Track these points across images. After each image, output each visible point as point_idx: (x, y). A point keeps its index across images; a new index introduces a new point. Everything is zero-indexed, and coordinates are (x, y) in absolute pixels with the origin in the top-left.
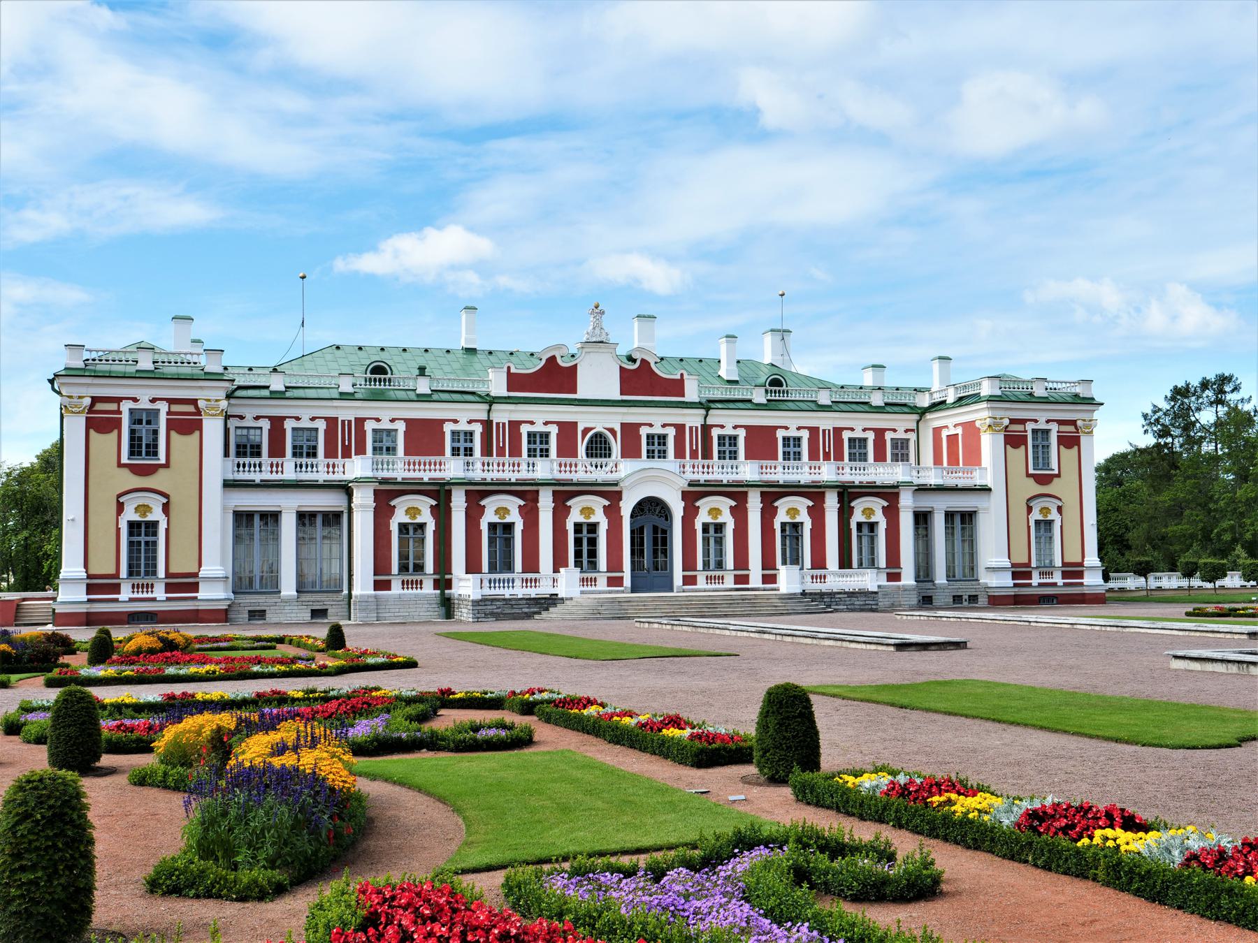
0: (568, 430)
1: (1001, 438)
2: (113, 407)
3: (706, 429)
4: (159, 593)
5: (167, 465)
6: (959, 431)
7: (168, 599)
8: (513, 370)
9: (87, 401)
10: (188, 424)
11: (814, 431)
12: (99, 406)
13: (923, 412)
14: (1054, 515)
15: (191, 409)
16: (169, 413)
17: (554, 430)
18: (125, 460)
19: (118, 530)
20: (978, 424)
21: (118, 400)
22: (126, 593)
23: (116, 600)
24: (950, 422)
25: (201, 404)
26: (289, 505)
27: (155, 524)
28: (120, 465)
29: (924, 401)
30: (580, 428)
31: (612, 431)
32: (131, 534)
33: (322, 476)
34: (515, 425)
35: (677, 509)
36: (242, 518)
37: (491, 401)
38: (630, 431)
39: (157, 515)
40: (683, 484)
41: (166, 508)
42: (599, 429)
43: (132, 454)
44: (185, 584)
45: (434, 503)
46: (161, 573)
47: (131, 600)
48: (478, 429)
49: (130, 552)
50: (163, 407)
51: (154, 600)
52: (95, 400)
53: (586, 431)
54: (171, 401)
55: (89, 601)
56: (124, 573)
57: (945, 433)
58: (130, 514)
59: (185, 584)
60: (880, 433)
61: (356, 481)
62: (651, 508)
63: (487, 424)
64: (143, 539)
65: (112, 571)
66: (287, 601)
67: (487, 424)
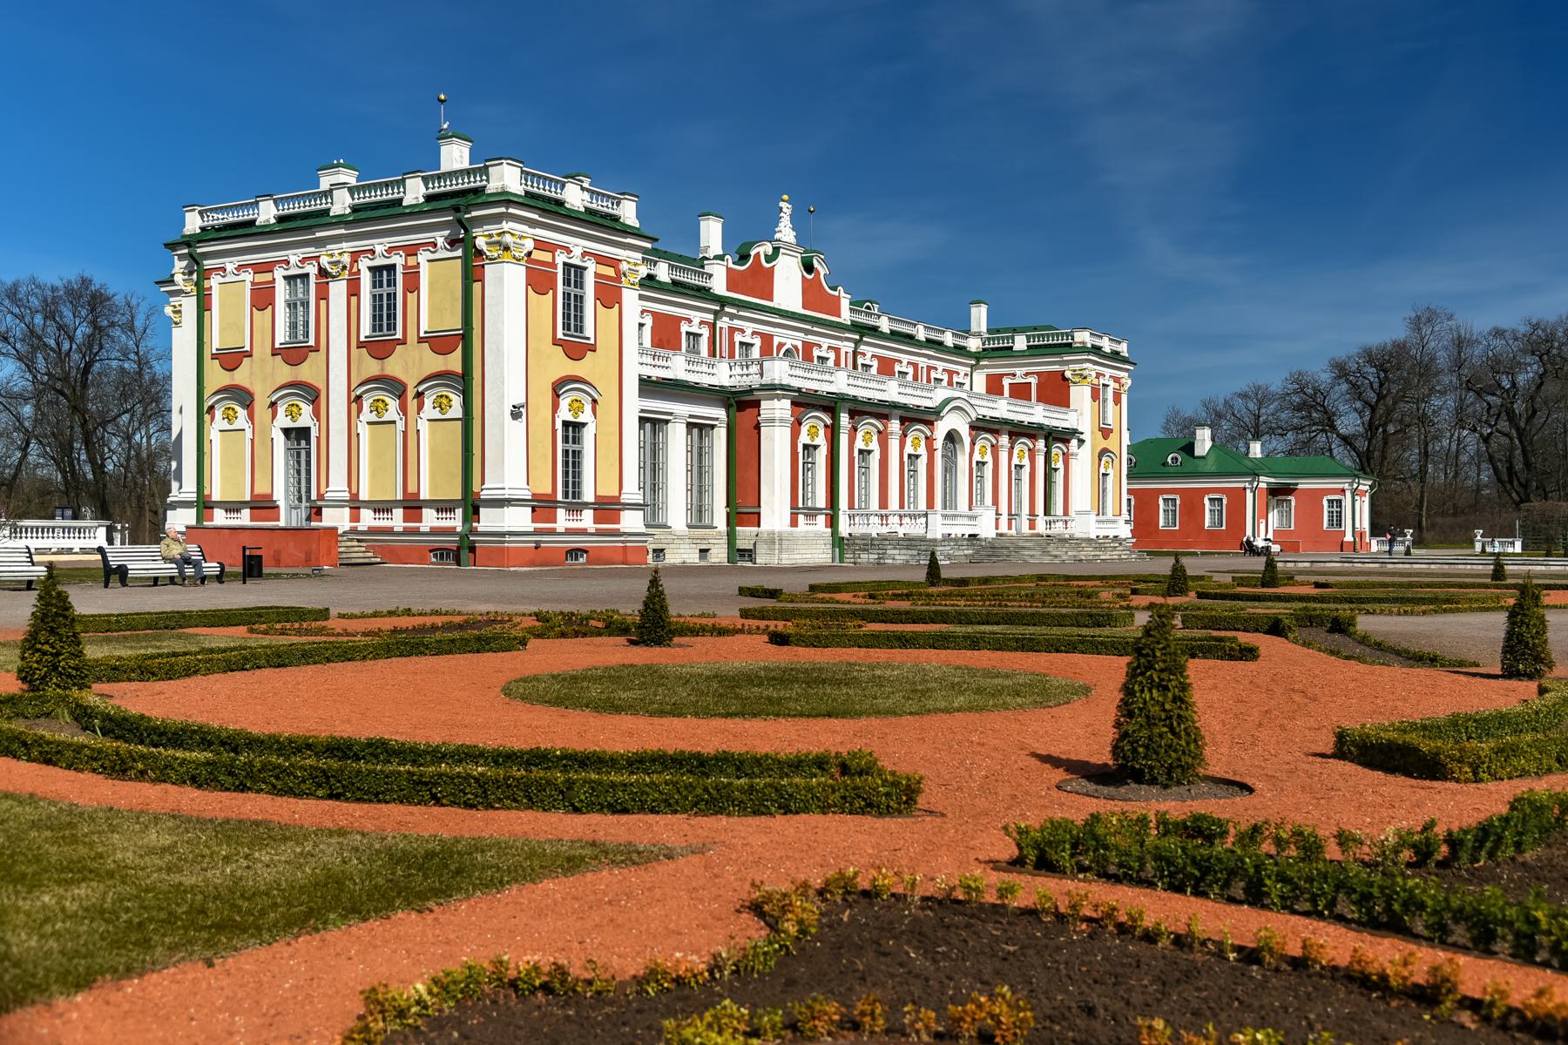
0: (767, 340)
1: (1087, 391)
2: (545, 257)
3: (855, 353)
4: (587, 520)
5: (593, 348)
6: (1033, 380)
7: (599, 533)
8: (731, 265)
9: (529, 245)
10: (609, 295)
11: (915, 366)
12: (537, 255)
13: (978, 357)
14: (1110, 471)
15: (610, 272)
16: (597, 275)
17: (757, 341)
18: (560, 335)
19: (554, 431)
20: (1068, 374)
21: (550, 247)
22: (563, 520)
23: (552, 532)
24: (1019, 371)
25: (624, 267)
26: (683, 410)
27: (584, 425)
28: (556, 342)
29: (974, 344)
30: (776, 341)
31: (796, 347)
32: (566, 440)
33: (705, 380)
34: (732, 330)
35: (967, 440)
36: (642, 421)
37: (722, 301)
38: (808, 347)
39: (586, 416)
40: (974, 416)
41: (595, 401)
42: (788, 346)
43: (566, 326)
44: (608, 508)
45: (829, 422)
46: (588, 495)
47: (569, 532)
48: (705, 332)
49: (566, 464)
50: (591, 267)
51: (583, 532)
52: (540, 245)
53: (781, 345)
54: (601, 260)
55: (537, 532)
56: (560, 497)
57: (1006, 382)
58: (564, 414)
59: (608, 508)
60: (951, 373)
61: (772, 387)
62: (952, 437)
63: (713, 326)
64: (571, 447)
65: (549, 491)
66: (680, 538)
67: (713, 326)
